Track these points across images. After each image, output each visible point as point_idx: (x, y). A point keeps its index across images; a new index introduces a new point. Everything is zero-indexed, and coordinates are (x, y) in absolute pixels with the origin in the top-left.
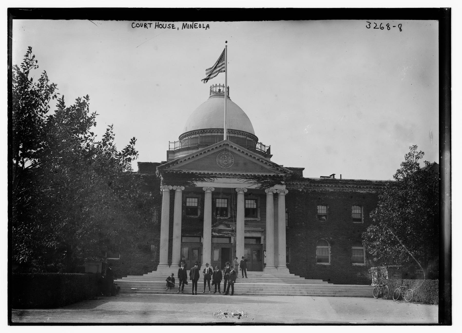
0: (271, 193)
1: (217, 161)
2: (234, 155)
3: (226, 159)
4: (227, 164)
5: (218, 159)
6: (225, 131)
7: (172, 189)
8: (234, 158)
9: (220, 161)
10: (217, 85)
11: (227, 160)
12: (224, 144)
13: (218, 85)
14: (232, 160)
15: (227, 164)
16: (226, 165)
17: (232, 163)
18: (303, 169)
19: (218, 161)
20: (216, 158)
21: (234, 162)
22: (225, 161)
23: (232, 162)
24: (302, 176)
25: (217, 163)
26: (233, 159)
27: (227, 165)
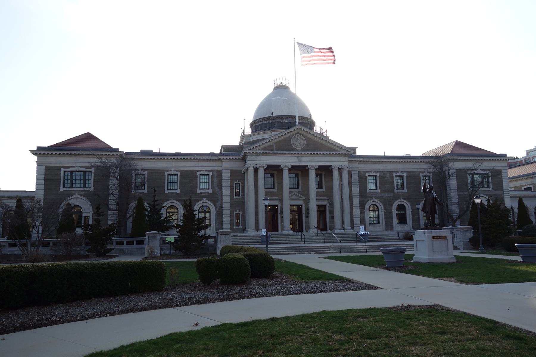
0: (337, 169)
6: (297, 118)
7: (256, 167)
9: (294, 142)
11: (300, 142)
12: (298, 128)
15: (299, 145)
17: (304, 144)
18: (357, 147)
24: (356, 154)
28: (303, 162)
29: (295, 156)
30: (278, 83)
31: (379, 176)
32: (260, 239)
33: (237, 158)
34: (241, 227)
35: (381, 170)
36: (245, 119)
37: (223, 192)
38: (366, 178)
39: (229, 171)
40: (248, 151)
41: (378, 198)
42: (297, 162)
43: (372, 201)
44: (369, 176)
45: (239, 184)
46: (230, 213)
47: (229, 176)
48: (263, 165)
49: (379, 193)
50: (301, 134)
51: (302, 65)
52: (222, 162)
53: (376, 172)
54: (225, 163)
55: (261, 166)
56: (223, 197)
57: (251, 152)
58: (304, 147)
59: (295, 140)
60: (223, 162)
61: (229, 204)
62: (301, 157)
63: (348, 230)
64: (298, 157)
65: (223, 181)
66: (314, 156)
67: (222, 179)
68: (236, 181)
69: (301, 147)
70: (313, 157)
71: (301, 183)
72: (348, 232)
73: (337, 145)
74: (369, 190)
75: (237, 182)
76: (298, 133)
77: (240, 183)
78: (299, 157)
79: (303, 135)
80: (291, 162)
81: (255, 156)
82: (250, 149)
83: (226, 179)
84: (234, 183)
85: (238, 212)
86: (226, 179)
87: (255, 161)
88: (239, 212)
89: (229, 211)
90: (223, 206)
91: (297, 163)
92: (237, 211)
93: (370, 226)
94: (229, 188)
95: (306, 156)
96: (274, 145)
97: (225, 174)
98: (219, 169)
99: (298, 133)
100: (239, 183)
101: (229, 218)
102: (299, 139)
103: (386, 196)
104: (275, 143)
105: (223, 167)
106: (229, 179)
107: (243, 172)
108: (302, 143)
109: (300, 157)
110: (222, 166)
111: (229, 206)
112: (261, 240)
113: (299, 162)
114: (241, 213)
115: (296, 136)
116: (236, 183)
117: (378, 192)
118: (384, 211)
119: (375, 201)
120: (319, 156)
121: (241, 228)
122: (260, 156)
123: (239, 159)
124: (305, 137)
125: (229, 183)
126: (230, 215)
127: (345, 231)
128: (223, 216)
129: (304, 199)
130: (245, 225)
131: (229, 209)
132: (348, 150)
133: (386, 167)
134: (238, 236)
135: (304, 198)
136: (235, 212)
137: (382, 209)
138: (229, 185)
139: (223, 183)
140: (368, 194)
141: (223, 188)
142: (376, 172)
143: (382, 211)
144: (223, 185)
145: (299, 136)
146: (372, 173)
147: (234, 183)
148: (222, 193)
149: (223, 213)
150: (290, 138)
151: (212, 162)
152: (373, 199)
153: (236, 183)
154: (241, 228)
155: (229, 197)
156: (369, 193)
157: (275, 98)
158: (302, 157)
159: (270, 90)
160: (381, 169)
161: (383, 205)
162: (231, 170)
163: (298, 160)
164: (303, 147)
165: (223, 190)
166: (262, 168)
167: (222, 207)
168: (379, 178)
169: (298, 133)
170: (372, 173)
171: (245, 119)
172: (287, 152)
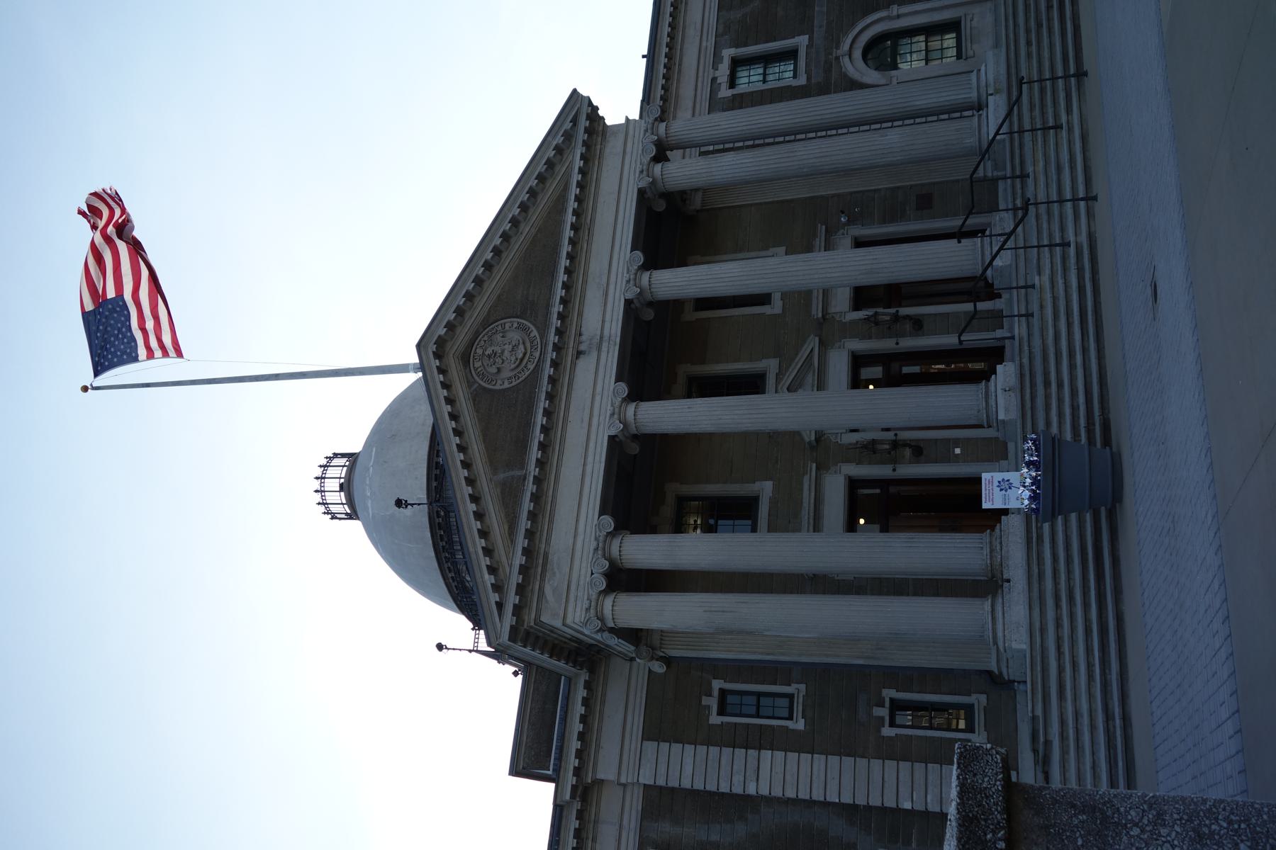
1: (506, 385)
4: (524, 343)
5: (499, 382)
9: (506, 374)
10: (319, 489)
11: (506, 346)
13: (316, 484)
15: (521, 347)
16: (525, 349)
17: (521, 328)
20: (490, 390)
21: (517, 317)
22: (507, 354)
23: (515, 325)
25: (514, 384)
26: (503, 326)
27: (528, 345)
28: (607, 325)
29: (574, 365)
30: (336, 498)
31: (737, 46)
32: (1073, 516)
33: (581, 693)
34: (979, 700)
35: (710, 43)
36: (440, 647)
37: (764, 791)
38: (742, 95)
39: (650, 746)
40: (509, 619)
41: (834, 39)
42: (603, 355)
43: (846, 59)
44: (732, 85)
45: (723, 693)
46: (890, 764)
47: (677, 747)
48: (596, 539)
49: (811, 39)
50: (471, 344)
51: (179, 354)
52: (601, 782)
53: (717, 58)
54: (606, 770)
55: (602, 549)
56: (790, 794)
57: (512, 599)
58: (534, 325)
59: (493, 370)
60: (600, 776)
61: (834, 760)
62: (584, 338)
63: (991, 77)
64: (579, 354)
65: (699, 785)
66: (585, 274)
67: (693, 793)
68: (708, 707)
69: (532, 343)
70: (590, 280)
71: (737, 360)
72: (1003, 78)
73: (541, 167)
74: (795, 76)
75: (713, 702)
76: (465, 359)
77: (717, 685)
78: (582, 348)
79: (477, 334)
80: (599, 389)
81: (542, 579)
82: (500, 606)
83: (688, 769)
84: (715, 719)
85: (883, 712)
86: (688, 769)
87: (573, 587)
88: (883, 706)
89: (876, 764)
90: (847, 799)
91: (611, 358)
92: (882, 718)
93: (970, 53)
94: (740, 752)
95: (580, 314)
96: (501, 476)
97: (662, 769)
98: (635, 803)
99: (465, 359)
100: (716, 693)
101: (919, 767)
102: (489, 352)
103: (825, 9)
104: (495, 470)
105: (623, 780)
106: (689, 749)
107: (659, 668)
108: (515, 336)
110: (624, 785)
111: (848, 761)
112: (1073, 516)
113: (605, 345)
114: (888, 693)
115: (478, 364)
116: (721, 712)
117: (806, 42)
118: (895, 10)
119: (846, 47)
120: (588, 251)
121: (983, 698)
122: (546, 555)
123: (588, 685)
124: (486, 323)
125: (714, 750)
126: (904, 766)
127: (997, 91)
128: (907, 805)
129: (821, 342)
130: (966, 674)
131: (862, 762)
132: (570, 117)
133: (699, 26)
134: (1039, 712)
135: (813, 343)
136: (887, 731)
137: (889, 18)
138: (727, 751)
139: (711, 787)
140: (813, 81)
141: (738, 790)
142: (717, 58)
143: (895, 13)
144: (724, 788)
145: (480, 351)
146: (717, 74)
147: (715, 719)
148: (769, 800)
149: (890, 803)
150: (480, 396)
151: (594, 840)
152: (837, 58)
153: (721, 712)
154: (983, 698)
155: (793, 756)
156: (809, 79)
157: (369, 503)
158: (580, 335)
159: (356, 528)
160: (704, 44)
161: (866, 13)
162: (646, 737)
163: (595, 354)
164: (535, 333)
165: (751, 790)
166: (616, 543)
167: (853, 808)
168: (746, 45)
170: (717, 74)
171: (440, 647)
172: (542, 404)
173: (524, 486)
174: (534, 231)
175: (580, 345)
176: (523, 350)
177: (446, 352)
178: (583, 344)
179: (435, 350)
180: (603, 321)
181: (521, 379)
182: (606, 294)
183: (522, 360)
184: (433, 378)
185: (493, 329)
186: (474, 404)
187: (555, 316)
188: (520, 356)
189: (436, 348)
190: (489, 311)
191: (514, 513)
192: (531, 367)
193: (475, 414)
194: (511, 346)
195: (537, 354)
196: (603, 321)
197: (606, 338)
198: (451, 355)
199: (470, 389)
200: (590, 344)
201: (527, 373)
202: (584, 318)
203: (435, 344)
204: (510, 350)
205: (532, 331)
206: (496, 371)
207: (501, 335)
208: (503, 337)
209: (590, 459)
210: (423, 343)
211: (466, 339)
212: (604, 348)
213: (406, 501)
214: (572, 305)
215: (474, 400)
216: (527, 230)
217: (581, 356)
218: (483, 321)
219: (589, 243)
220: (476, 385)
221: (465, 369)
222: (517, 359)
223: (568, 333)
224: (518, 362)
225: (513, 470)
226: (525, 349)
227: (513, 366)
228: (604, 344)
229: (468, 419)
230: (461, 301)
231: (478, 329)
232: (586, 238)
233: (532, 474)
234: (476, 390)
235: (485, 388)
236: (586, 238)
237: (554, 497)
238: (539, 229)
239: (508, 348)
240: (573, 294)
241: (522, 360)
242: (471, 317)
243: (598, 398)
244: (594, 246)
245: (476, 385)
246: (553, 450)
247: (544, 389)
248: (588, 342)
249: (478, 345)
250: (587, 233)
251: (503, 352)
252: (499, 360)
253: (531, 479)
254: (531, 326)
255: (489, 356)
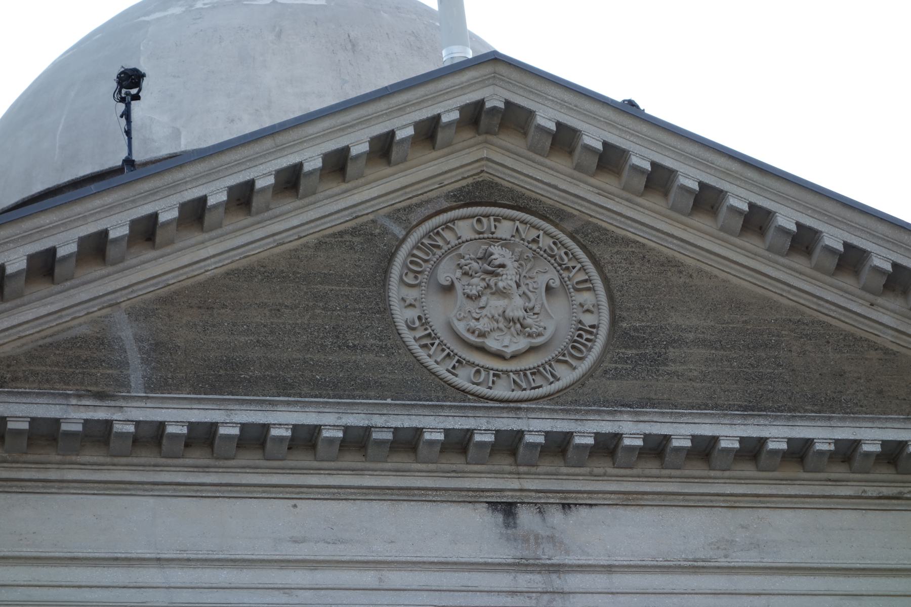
1: (402, 315)
2: (596, 251)
3: (507, 279)
4: (532, 349)
5: (412, 295)
8: (606, 281)
11: (519, 302)
14: (586, 298)
15: (522, 343)
16: (514, 356)
19: (412, 314)
20: (386, 272)
21: (614, 321)
22: (496, 304)
23: (588, 319)
25: (408, 336)
26: (586, 286)
29: (470, 497)
42: (503, 581)
58: (590, 374)
59: (446, 273)
62: (556, 517)
66: (758, 501)
69: (536, 372)
70: (743, 516)
78: (526, 517)
80: (396, 578)
95: (629, 500)
102: (499, 254)
104: (141, 313)
109: (541, 509)
113: (536, 581)
115: (465, 229)
120: (830, 502)
145: (505, 230)
158: (566, 506)
163: (505, 553)
164: (566, 376)
169: (492, 186)
173: (79, 396)
174: (887, 339)
175: (534, 510)
176: (509, 351)
177: (490, 138)
178: (537, 518)
179: (488, 105)
180: (609, 569)
181: (422, 354)
182: (695, 568)
183: (482, 350)
184: (401, 110)
185: (575, 257)
186: (341, 234)
187: (607, 427)
188: (492, 343)
189: (494, 109)
190: (627, 242)
191: (15, 379)
192: (463, 379)
193: (312, 239)
194: (520, 313)
195: (501, 390)
196: (609, 569)
197: (557, 582)
198: (485, 153)
199: (388, 216)
200: (537, 537)
201: (441, 370)
202: (621, 511)
203: (508, 103)
204: (510, 314)
205: (574, 368)
206: (444, 279)
207: (556, 283)
208: (549, 289)
209: (179, 576)
210: (502, 69)
211: (540, 189)
212: (524, 581)
213: (137, 97)
214: (655, 472)
215: (354, 232)
216: (886, 319)
217: (500, 518)
218: (599, 229)
219: (859, 502)
220: (399, 232)
221: (447, 196)
222: (482, 335)
223: (564, 470)
224: (472, 338)
225: (144, 361)
226: (514, 356)
227: (461, 327)
228: (537, 578)
229: (295, 222)
230: (643, 158)
231: (572, 216)
232: (872, 491)
233: (117, 416)
234: (385, 231)
235: (391, 257)
236: (872, 491)
237: (63, 485)
238: (895, 353)
239: (515, 306)
240: (687, 472)
241: (482, 350)
242: (602, 192)
243: (368, 578)
244: (848, 518)
245: (399, 232)
246: (205, 469)
247: (378, 421)
248: (543, 532)
249: (523, 222)
250: (886, 491)
251: (502, 293)
252: (476, 284)
253: (101, 415)
254: (583, 367)
255: (486, 257)
